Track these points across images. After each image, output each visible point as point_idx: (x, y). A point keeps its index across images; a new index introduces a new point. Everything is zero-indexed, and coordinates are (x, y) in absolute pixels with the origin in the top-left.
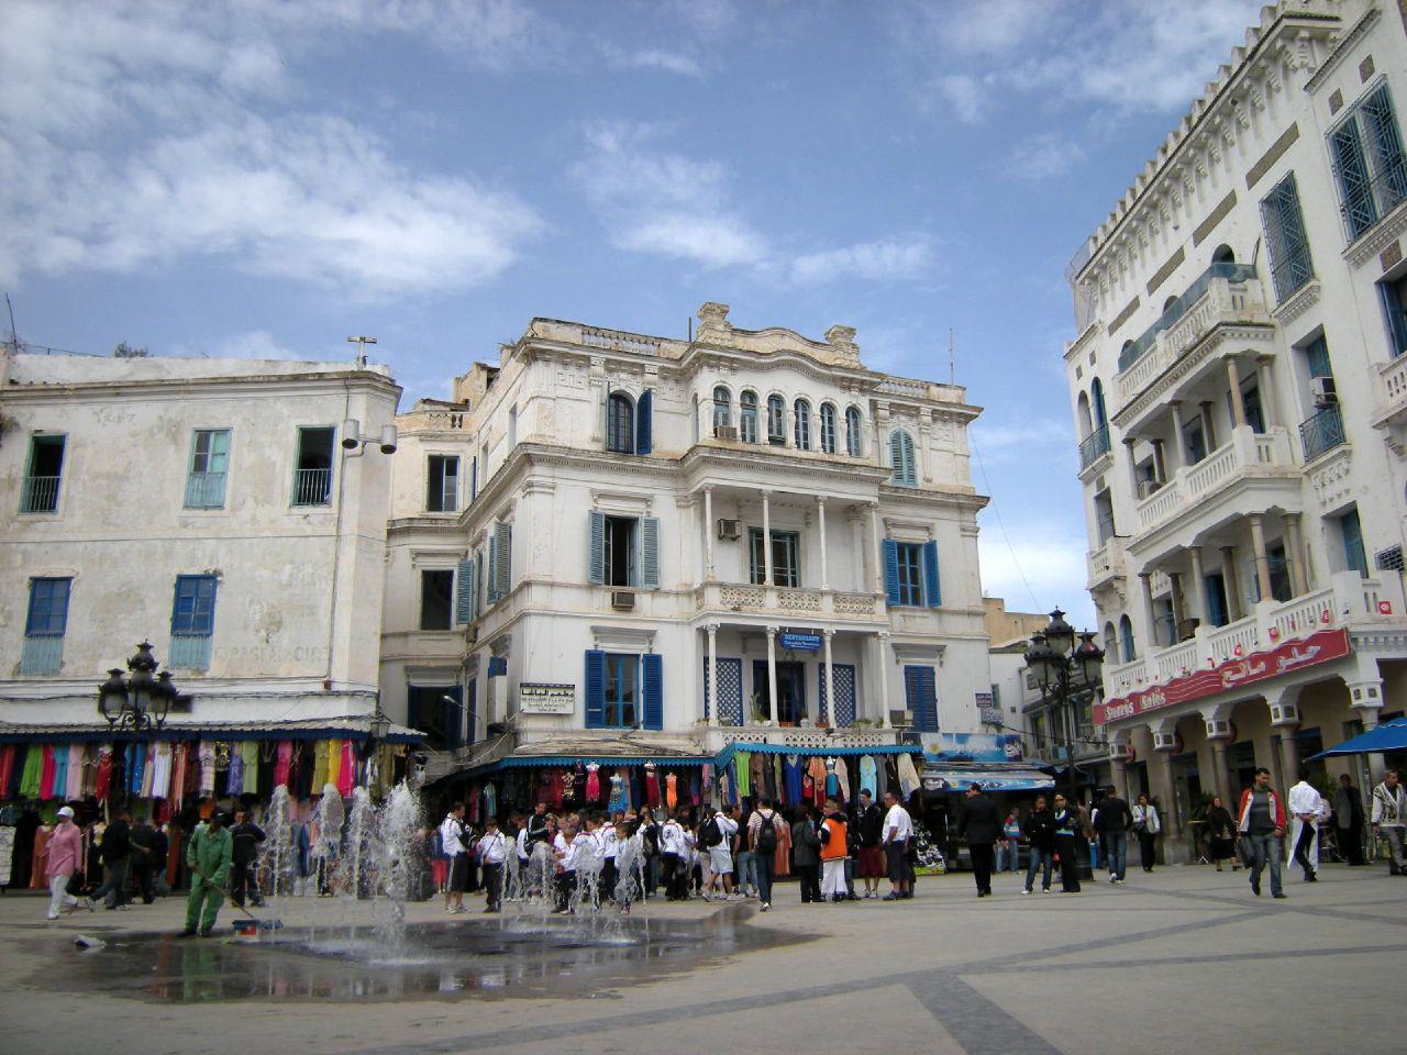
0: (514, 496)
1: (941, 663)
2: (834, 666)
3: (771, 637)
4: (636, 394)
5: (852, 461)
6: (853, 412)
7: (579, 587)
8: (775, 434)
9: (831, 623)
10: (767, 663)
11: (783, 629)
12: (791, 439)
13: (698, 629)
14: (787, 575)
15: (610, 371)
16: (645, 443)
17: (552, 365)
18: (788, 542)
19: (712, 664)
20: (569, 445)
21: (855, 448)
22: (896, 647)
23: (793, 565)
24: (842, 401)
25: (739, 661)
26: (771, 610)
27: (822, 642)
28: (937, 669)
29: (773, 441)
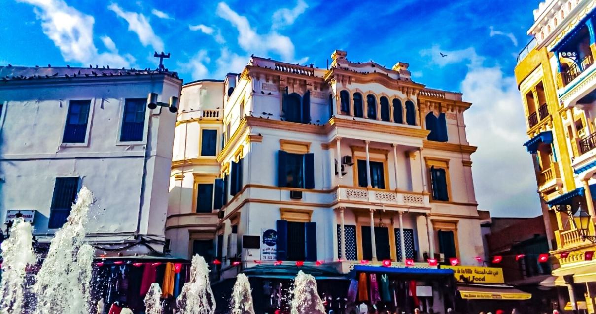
21: (411, 121)
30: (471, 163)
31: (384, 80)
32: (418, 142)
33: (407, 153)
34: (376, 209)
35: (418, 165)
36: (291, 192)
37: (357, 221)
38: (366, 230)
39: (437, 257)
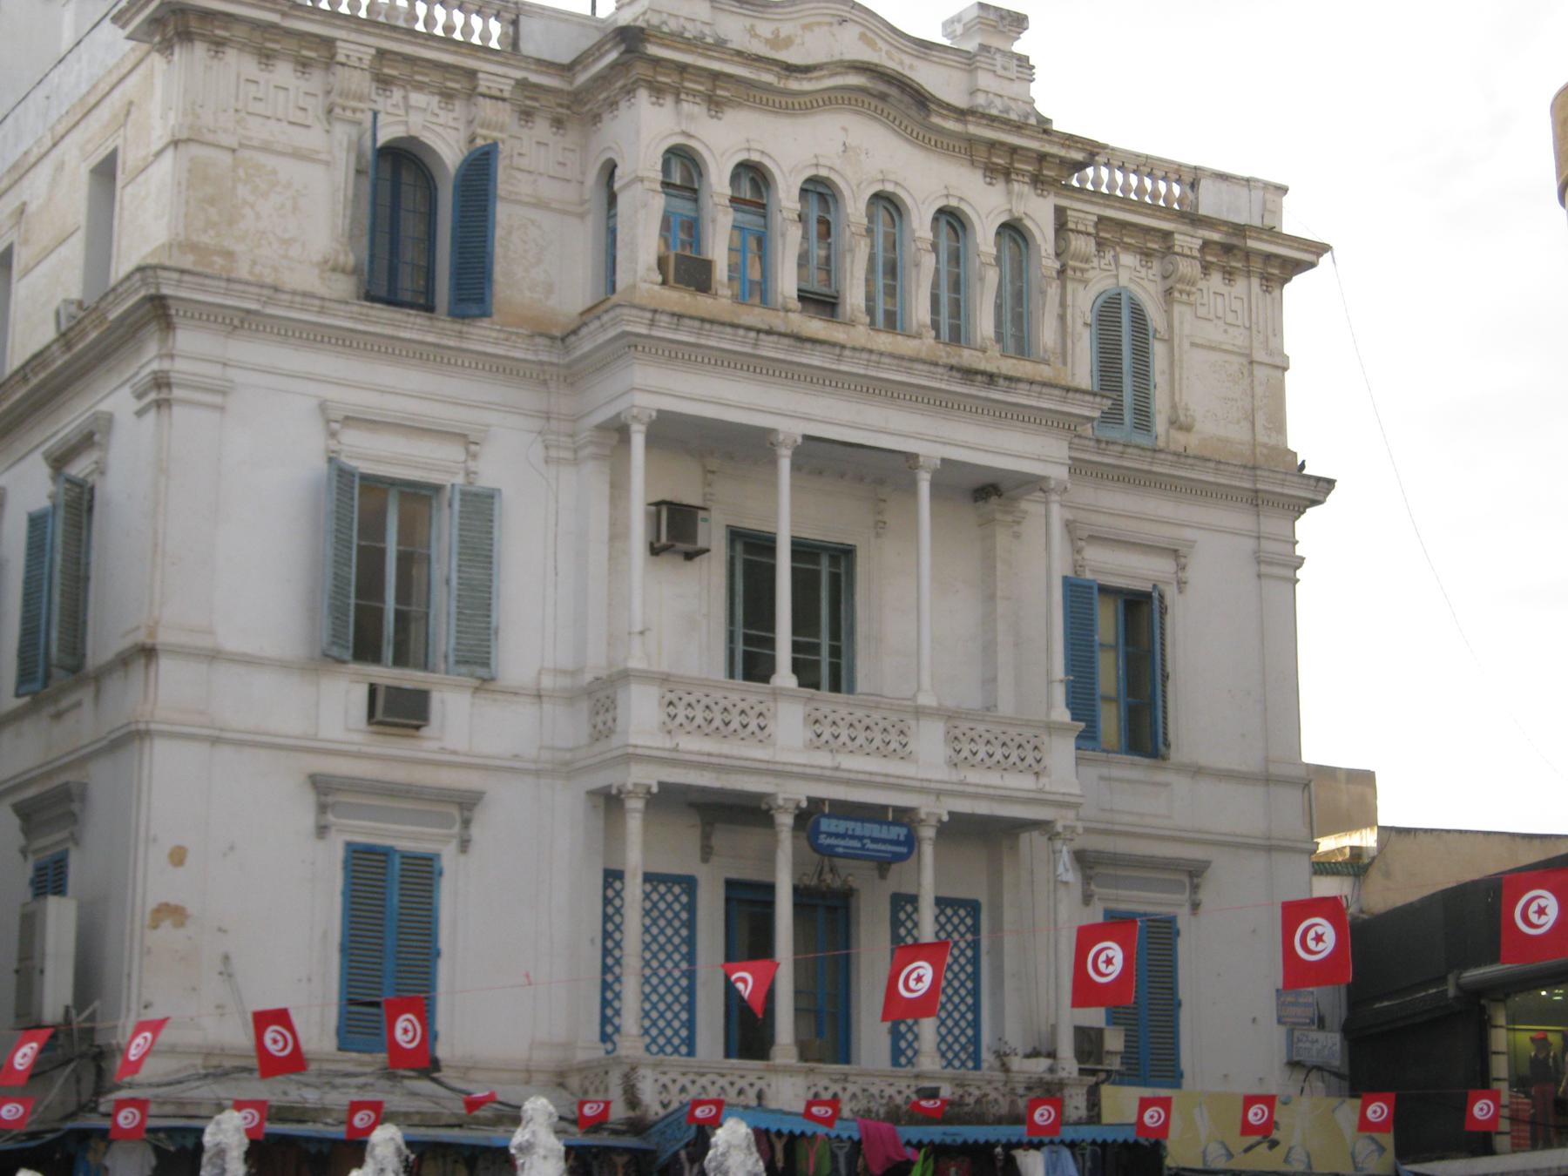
0: (104, 407)
1: (1195, 906)
2: (940, 902)
3: (785, 820)
4: (449, 150)
5: (1009, 366)
6: (1013, 231)
7: (283, 665)
8: (816, 285)
9: (939, 794)
10: (770, 888)
11: (816, 803)
12: (854, 296)
13: (592, 793)
14: (827, 665)
15: (384, 82)
16: (473, 292)
17: (231, 55)
18: (825, 568)
19: (634, 889)
20: (269, 280)
22: (1082, 859)
23: (835, 634)
24: (988, 207)
26: (788, 744)
27: (911, 842)
28: (1184, 922)
29: (804, 297)
30: (1300, 562)
33: (986, 493)
34: (661, 784)
36: (373, 690)
37: (707, 853)
38: (749, 908)
39: (1088, 1043)
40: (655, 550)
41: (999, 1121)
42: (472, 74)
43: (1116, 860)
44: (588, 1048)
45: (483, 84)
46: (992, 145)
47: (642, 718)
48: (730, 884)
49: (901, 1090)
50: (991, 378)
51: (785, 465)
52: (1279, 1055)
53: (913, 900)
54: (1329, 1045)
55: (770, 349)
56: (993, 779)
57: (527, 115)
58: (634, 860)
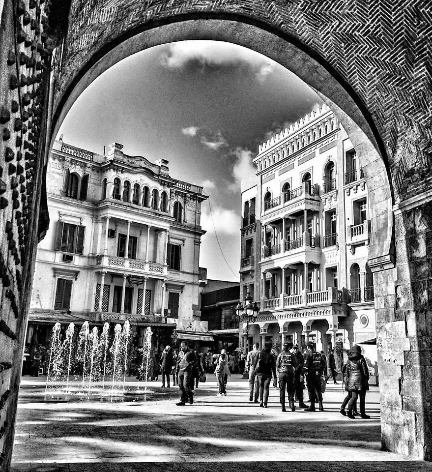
4: (81, 174)
6: (164, 194)
9: (147, 275)
10: (122, 287)
12: (141, 201)
19: (102, 287)
20: (53, 193)
22: (166, 285)
24: (161, 189)
25: (109, 286)
26: (126, 267)
27: (143, 282)
31: (149, 173)
32: (165, 225)
33: (157, 231)
35: (163, 240)
36: (64, 255)
37: (112, 281)
38: (118, 290)
39: (166, 311)
40: (108, 236)
41: (152, 323)
42: (86, 164)
43: (171, 285)
44: (93, 310)
45: (87, 165)
46: (162, 180)
47: (105, 262)
48: (115, 286)
49: (138, 317)
50: (160, 215)
51: (149, 230)
52: (192, 314)
53: (143, 290)
54: (199, 313)
55: (128, 209)
56: (155, 273)
57: (93, 170)
58: (103, 283)
